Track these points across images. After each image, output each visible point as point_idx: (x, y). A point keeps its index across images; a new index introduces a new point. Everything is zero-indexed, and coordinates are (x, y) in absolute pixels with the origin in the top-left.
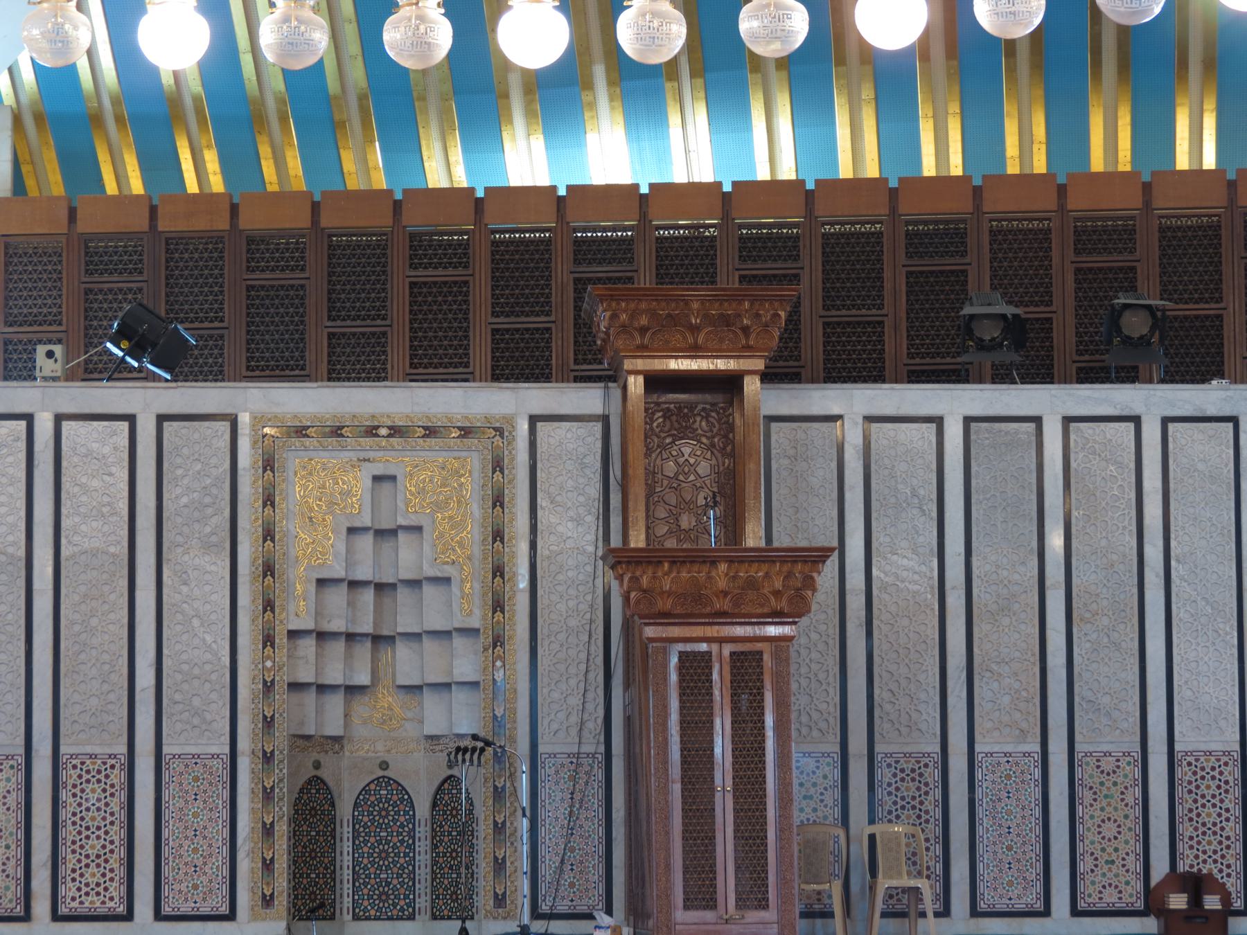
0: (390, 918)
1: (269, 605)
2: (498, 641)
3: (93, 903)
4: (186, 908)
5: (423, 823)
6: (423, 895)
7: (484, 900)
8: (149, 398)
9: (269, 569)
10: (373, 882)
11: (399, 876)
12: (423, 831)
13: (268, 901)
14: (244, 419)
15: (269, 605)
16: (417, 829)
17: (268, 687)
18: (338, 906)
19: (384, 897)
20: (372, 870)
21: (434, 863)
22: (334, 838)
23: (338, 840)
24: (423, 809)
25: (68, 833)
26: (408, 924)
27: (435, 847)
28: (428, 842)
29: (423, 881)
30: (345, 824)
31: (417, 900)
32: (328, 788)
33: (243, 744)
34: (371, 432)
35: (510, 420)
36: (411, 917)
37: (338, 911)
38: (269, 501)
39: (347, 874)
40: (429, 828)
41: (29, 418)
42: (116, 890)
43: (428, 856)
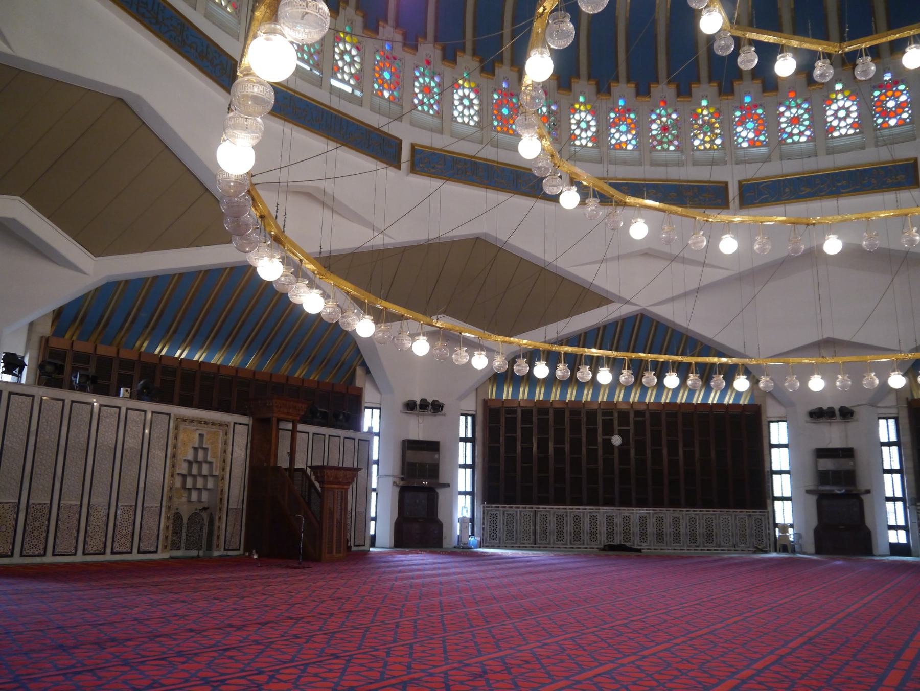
1: (173, 466)
2: (223, 479)
3: (122, 549)
4: (146, 550)
7: (214, 546)
8: (149, 407)
9: (174, 456)
12: (185, 526)
13: (166, 547)
14: (172, 416)
15: (173, 466)
17: (171, 488)
24: (185, 521)
25: (118, 528)
33: (164, 504)
34: (200, 422)
35: (229, 423)
38: (176, 438)
41: (119, 408)
42: (129, 545)
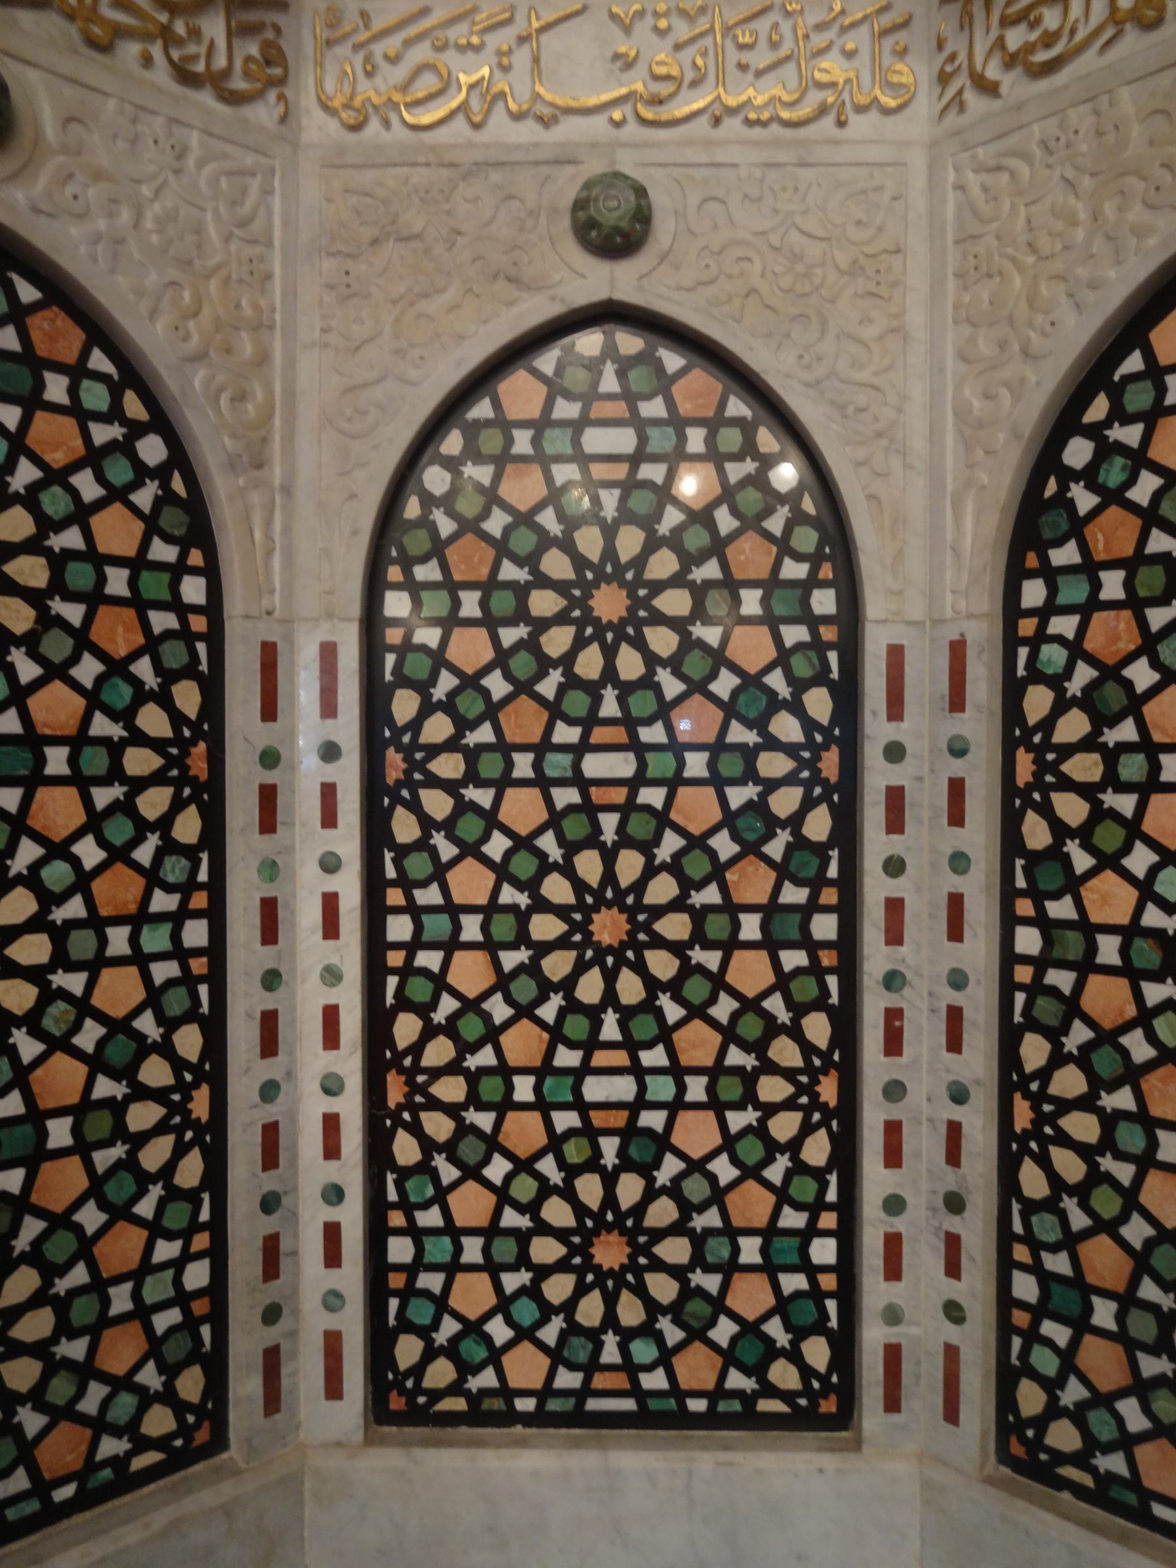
0: (662, 1417)
5: (926, 676)
6: (922, 1258)
10: (525, 1132)
11: (729, 1089)
16: (877, 730)
18: (245, 1344)
19: (610, 1253)
20: (522, 1043)
21: (1029, 1006)
22: (210, 799)
23: (241, 809)
26: (787, 1473)
27: (1032, 875)
28: (980, 835)
29: (922, 1144)
30: (303, 689)
31: (875, 1291)
32: (132, 375)
36: (826, 1410)
37: (245, 1386)
39: (322, 1083)
40: (980, 722)
43: (978, 951)
